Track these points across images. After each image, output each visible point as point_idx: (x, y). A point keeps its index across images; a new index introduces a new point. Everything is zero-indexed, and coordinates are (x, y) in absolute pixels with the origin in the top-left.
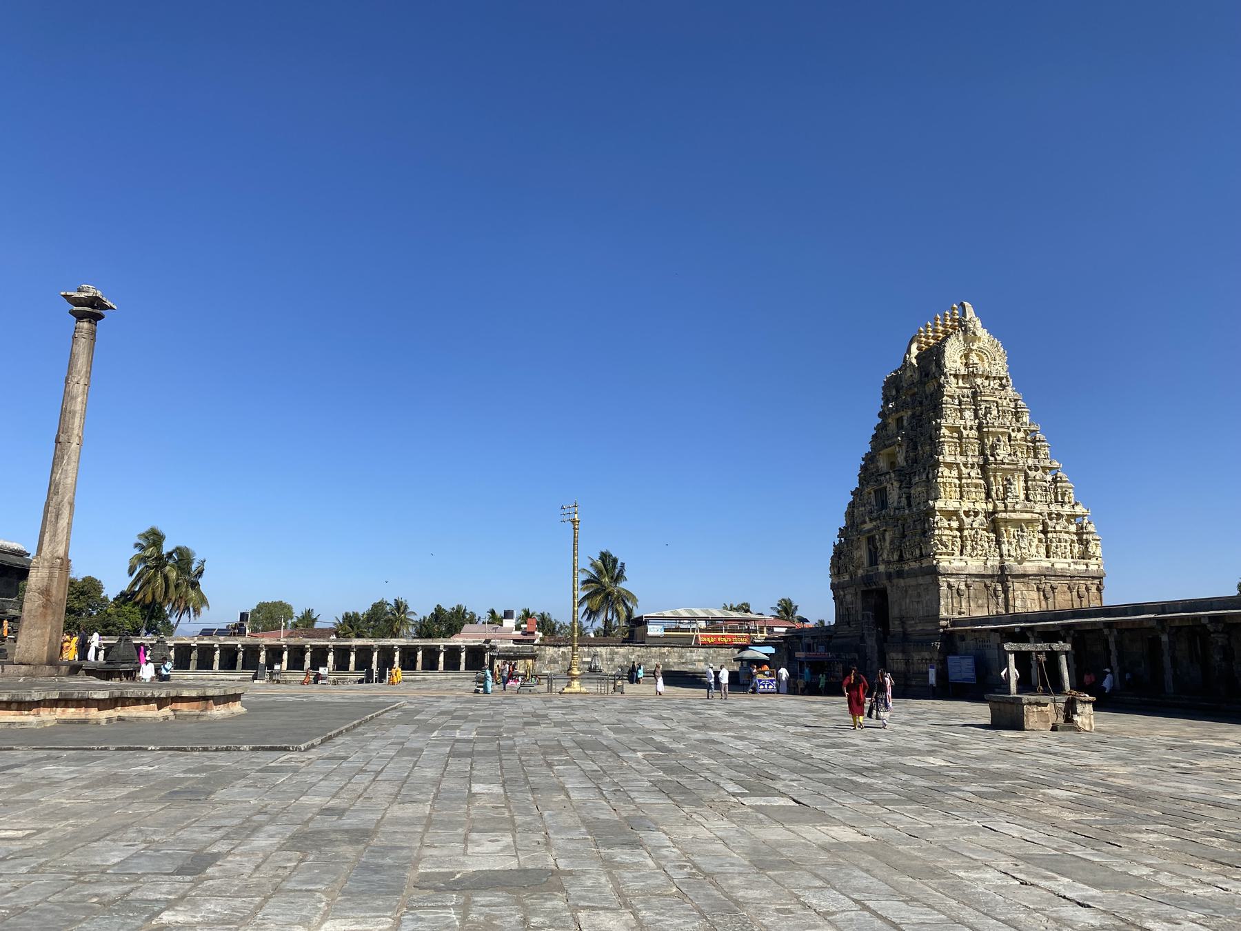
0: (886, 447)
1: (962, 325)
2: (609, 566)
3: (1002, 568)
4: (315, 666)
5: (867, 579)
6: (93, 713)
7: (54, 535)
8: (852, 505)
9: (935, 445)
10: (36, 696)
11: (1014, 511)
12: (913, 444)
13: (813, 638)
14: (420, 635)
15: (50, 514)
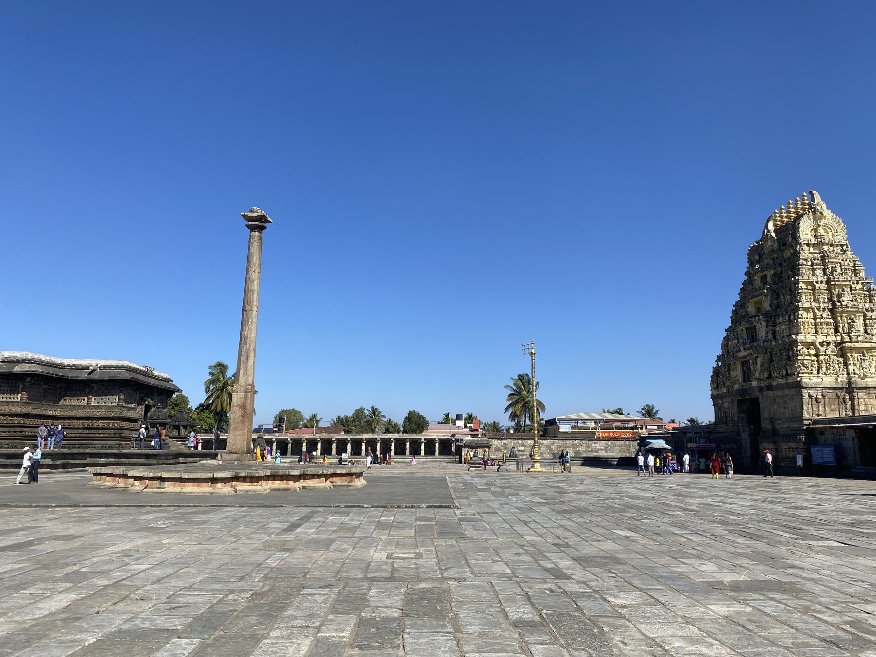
0: (754, 297)
1: (812, 208)
2: (524, 383)
3: (849, 382)
4: (339, 453)
5: (742, 392)
6: (291, 484)
7: (246, 370)
8: (726, 339)
9: (794, 295)
10: (262, 473)
11: (857, 342)
12: (776, 295)
13: (696, 433)
14: (405, 432)
15: (242, 356)
